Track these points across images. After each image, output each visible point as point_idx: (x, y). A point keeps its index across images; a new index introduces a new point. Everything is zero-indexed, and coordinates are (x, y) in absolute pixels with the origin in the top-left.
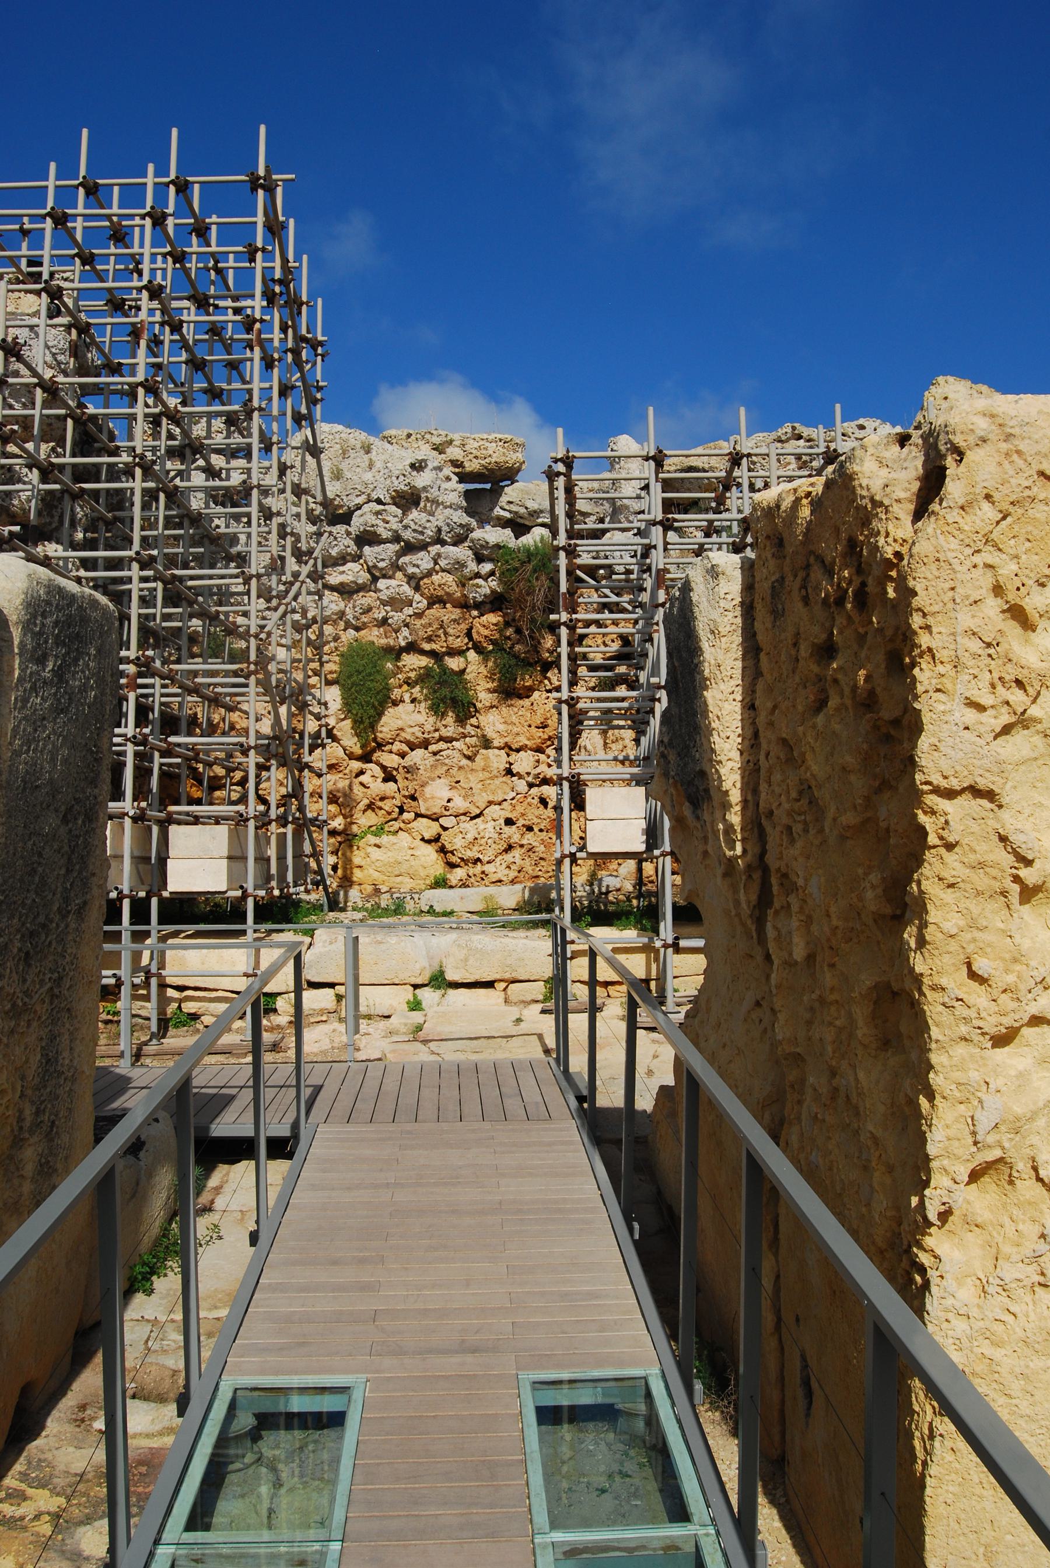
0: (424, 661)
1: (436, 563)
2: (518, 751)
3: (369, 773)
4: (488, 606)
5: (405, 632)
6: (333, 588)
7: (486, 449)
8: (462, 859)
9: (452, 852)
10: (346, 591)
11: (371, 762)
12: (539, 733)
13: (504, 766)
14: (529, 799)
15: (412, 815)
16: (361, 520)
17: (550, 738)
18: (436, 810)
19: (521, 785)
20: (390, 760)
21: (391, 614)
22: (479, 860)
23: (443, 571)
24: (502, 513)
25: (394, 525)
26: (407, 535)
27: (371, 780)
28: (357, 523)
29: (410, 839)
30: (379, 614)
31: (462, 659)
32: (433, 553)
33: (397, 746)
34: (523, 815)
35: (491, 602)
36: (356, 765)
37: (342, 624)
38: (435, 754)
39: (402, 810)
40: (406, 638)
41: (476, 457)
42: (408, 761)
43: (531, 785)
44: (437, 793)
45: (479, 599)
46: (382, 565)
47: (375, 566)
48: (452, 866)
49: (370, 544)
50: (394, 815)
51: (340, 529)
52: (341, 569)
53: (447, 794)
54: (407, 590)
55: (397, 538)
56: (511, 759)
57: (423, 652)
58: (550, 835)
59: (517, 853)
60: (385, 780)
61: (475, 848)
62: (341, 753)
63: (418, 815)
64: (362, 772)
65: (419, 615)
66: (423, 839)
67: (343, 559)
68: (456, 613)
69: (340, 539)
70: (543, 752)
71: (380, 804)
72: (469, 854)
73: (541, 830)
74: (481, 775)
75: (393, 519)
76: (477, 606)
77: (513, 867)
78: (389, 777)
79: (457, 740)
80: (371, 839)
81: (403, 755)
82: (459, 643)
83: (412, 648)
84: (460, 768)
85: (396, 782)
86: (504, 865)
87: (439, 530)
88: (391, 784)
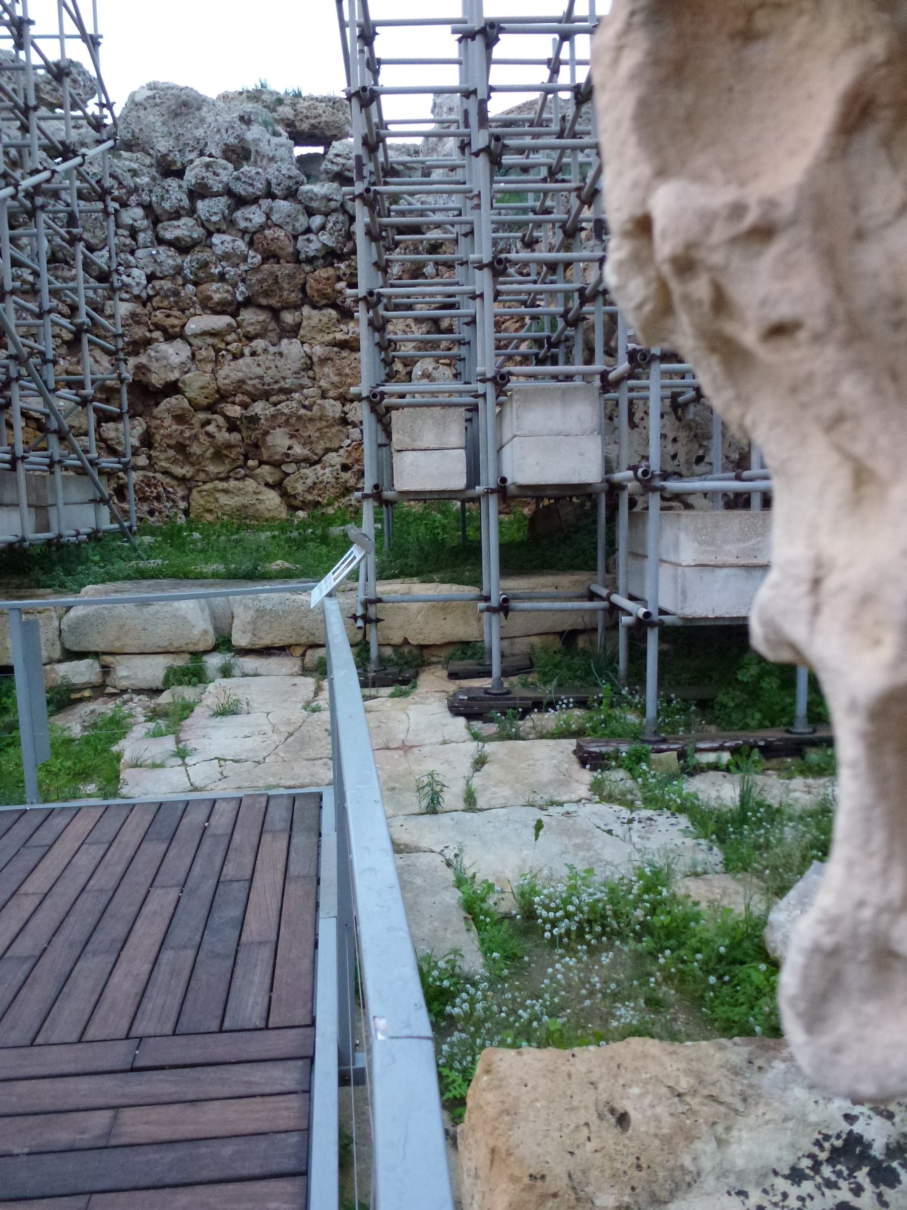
0: (262, 316)
1: (268, 217)
2: (352, 401)
4: (321, 261)
5: (242, 288)
6: (170, 244)
7: (315, 108)
10: (182, 247)
16: (193, 173)
18: (277, 457)
20: (234, 411)
21: (227, 269)
22: (318, 503)
23: (276, 225)
24: (330, 166)
25: (224, 176)
26: (240, 189)
27: (215, 430)
28: (190, 176)
29: (254, 484)
30: (215, 271)
31: (297, 313)
32: (264, 207)
35: (323, 257)
37: (180, 281)
39: (247, 458)
40: (242, 292)
41: (307, 117)
42: (250, 412)
44: (279, 440)
45: (312, 254)
46: (214, 219)
47: (208, 221)
48: (296, 509)
49: (203, 197)
50: (240, 463)
52: (176, 223)
53: (287, 442)
54: (241, 245)
55: (229, 192)
56: (346, 409)
57: (260, 307)
60: (230, 430)
61: (315, 492)
62: (186, 403)
63: (261, 463)
64: (208, 422)
65: (256, 269)
66: (267, 485)
67: (176, 215)
68: (289, 268)
69: (175, 193)
71: (225, 452)
72: (310, 498)
74: (318, 425)
75: (226, 173)
76: (310, 260)
78: (233, 426)
79: (295, 391)
81: (245, 406)
82: (294, 297)
83: (248, 302)
84: (299, 418)
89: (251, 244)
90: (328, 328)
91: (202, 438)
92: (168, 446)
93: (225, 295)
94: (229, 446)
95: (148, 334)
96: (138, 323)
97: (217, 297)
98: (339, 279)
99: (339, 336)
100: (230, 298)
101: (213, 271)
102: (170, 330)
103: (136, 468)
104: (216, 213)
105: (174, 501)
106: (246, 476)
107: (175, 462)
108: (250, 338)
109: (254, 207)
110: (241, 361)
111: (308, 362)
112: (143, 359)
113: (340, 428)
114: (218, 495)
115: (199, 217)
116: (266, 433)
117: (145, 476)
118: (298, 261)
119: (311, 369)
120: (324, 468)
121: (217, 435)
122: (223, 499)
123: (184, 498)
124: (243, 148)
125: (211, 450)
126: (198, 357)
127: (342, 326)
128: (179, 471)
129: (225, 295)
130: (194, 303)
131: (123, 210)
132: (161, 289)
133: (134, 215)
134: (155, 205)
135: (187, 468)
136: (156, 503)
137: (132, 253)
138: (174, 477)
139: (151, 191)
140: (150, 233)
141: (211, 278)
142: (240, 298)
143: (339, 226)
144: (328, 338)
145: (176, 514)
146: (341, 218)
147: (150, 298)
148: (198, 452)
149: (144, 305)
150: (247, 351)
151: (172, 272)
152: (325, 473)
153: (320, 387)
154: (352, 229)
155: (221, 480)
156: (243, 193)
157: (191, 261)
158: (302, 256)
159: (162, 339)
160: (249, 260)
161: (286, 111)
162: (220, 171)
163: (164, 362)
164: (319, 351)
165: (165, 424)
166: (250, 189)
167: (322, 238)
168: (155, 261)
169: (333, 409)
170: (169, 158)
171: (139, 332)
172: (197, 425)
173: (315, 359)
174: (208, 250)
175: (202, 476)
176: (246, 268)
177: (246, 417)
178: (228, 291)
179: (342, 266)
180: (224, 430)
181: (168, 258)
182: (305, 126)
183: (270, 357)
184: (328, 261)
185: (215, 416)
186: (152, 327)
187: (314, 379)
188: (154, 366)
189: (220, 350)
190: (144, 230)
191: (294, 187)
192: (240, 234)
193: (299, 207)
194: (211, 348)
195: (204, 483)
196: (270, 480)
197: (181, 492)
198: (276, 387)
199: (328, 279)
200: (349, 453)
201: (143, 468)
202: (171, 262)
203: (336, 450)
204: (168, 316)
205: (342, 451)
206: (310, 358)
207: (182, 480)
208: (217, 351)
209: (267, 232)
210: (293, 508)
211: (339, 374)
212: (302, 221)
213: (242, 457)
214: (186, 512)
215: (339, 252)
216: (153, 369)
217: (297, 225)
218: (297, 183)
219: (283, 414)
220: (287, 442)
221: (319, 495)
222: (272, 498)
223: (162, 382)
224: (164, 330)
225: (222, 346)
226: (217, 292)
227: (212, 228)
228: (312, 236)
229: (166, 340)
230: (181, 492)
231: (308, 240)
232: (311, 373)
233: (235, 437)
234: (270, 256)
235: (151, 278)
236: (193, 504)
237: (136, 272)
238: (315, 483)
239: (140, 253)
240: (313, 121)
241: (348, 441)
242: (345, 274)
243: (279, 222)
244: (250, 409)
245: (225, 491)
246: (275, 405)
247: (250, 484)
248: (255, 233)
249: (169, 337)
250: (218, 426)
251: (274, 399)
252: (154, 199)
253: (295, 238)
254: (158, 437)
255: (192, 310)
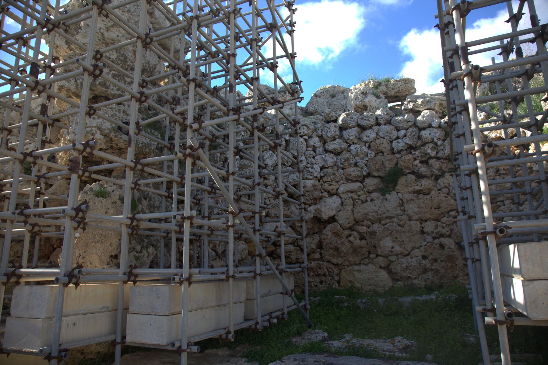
0: (376, 181)
1: (377, 134)
2: (426, 221)
3: (353, 236)
5: (365, 168)
6: (331, 152)
7: (396, 85)
8: (401, 277)
9: (395, 273)
10: (337, 153)
11: (353, 230)
12: (437, 211)
13: (419, 229)
14: (434, 245)
15: (374, 256)
17: (442, 213)
19: (429, 239)
20: (363, 229)
26: (362, 123)
29: (374, 267)
30: (352, 162)
33: (366, 222)
34: (431, 254)
35: (406, 150)
36: (347, 232)
38: (384, 225)
39: (369, 253)
43: (434, 238)
44: (387, 243)
46: (351, 138)
47: (349, 139)
50: (366, 256)
51: (332, 125)
52: (333, 142)
53: (390, 244)
54: (365, 149)
55: (359, 126)
56: (423, 225)
57: (375, 177)
58: (447, 263)
59: (430, 274)
60: (361, 239)
61: (408, 271)
63: (377, 255)
64: (350, 235)
66: (380, 267)
67: (334, 139)
68: (390, 156)
70: (439, 221)
71: (358, 250)
73: (442, 261)
76: (399, 152)
77: (428, 281)
79: (394, 217)
80: (356, 268)
83: (369, 175)
84: (397, 231)
85: (366, 239)
86: (423, 280)
87: (377, 119)
88: (364, 241)
89: (369, 147)
90: (411, 184)
91: (347, 244)
92: (330, 248)
93: (357, 173)
94: (361, 247)
95: (321, 194)
96: (316, 189)
97: (353, 174)
98: (415, 159)
99: (418, 188)
100: (359, 174)
101: (351, 162)
102: (331, 191)
103: (314, 260)
104: (352, 135)
105: (332, 276)
106: (369, 262)
107: (333, 256)
108: (370, 193)
109: (370, 131)
110: (365, 204)
111: (401, 202)
112: (318, 206)
113: (420, 235)
114: (355, 273)
115: (344, 138)
116: (380, 240)
117: (318, 264)
118: (393, 153)
119: (402, 205)
120: (412, 258)
121: (354, 241)
122: (358, 275)
123: (337, 274)
124: (364, 105)
125: (352, 249)
126: (344, 204)
127: (418, 183)
128: (334, 261)
129: (357, 173)
130: (342, 178)
131: (309, 139)
132: (327, 173)
133: (315, 141)
134: (324, 135)
135: (340, 259)
136: (323, 278)
137: (314, 157)
138: (333, 264)
139: (322, 130)
140: (322, 148)
141: (350, 165)
142: (365, 174)
143: (413, 134)
144: (411, 189)
145: (333, 283)
146: (415, 129)
147: (321, 177)
148: (345, 251)
149: (319, 181)
150: (369, 199)
151: (332, 164)
152: (413, 261)
153: (408, 215)
154: (420, 134)
155: (356, 264)
156: (365, 125)
157: (341, 159)
158: (395, 150)
159: (327, 196)
160: (369, 155)
161: (383, 88)
162: (353, 116)
163: (328, 207)
164: (407, 196)
165: (329, 237)
166: (368, 122)
167: (405, 141)
168: (324, 160)
169: (416, 226)
170: (330, 115)
171: (317, 194)
172: (344, 237)
173: (404, 200)
174: (349, 153)
175: (347, 263)
176: (367, 159)
177: (369, 232)
178: (358, 171)
179: (417, 153)
180: (358, 239)
181: (330, 159)
182: (392, 93)
183: (380, 201)
184: (408, 151)
185: (353, 232)
186: (323, 191)
187: (404, 211)
188: (323, 209)
189: (355, 199)
190: (319, 147)
191: (389, 119)
192: (364, 144)
193: (393, 127)
194: (351, 199)
195: (348, 266)
196: (383, 265)
197: (336, 271)
198: (384, 216)
199: (409, 160)
200: (426, 249)
201: (318, 260)
202: (331, 160)
203: (419, 248)
204: (330, 185)
205: (422, 249)
206: (402, 200)
207: (337, 265)
208: (354, 200)
209: (377, 141)
210: (395, 280)
211: (418, 207)
212: (395, 134)
213: (367, 253)
214: (339, 282)
215: (414, 146)
216: (323, 210)
217: (392, 136)
218: (391, 116)
219: (388, 230)
220: (390, 244)
221: (410, 273)
222: (384, 275)
223: (327, 217)
224: (329, 192)
225: (357, 197)
226: (353, 171)
227: (351, 143)
228: (400, 140)
229: (329, 196)
230: (336, 271)
231: (398, 142)
232: (402, 208)
233: (363, 242)
234: (379, 152)
235: (322, 168)
236: (342, 277)
237: (315, 166)
238: (407, 266)
239: (317, 157)
240: (396, 90)
241: (425, 243)
242: (418, 157)
243: (382, 136)
244: (371, 228)
245: (359, 271)
246: (384, 225)
247: (371, 267)
248: (371, 142)
249: (331, 195)
250: (354, 237)
251: (383, 222)
252: (323, 133)
253: (391, 142)
254: (325, 243)
255: (342, 181)
